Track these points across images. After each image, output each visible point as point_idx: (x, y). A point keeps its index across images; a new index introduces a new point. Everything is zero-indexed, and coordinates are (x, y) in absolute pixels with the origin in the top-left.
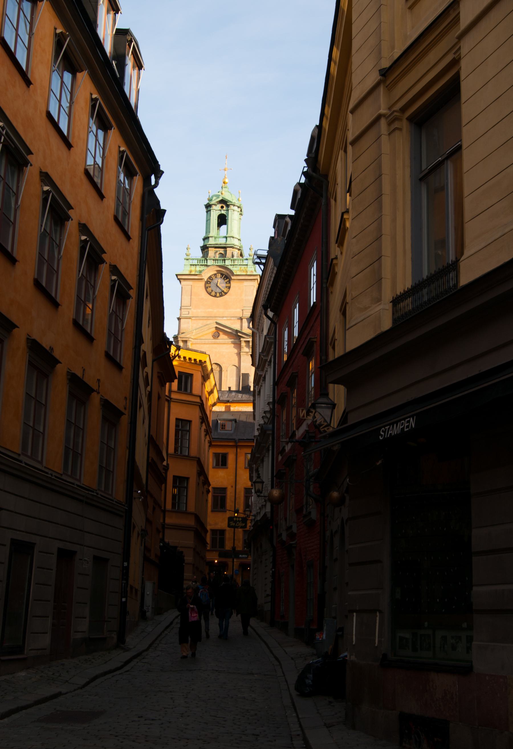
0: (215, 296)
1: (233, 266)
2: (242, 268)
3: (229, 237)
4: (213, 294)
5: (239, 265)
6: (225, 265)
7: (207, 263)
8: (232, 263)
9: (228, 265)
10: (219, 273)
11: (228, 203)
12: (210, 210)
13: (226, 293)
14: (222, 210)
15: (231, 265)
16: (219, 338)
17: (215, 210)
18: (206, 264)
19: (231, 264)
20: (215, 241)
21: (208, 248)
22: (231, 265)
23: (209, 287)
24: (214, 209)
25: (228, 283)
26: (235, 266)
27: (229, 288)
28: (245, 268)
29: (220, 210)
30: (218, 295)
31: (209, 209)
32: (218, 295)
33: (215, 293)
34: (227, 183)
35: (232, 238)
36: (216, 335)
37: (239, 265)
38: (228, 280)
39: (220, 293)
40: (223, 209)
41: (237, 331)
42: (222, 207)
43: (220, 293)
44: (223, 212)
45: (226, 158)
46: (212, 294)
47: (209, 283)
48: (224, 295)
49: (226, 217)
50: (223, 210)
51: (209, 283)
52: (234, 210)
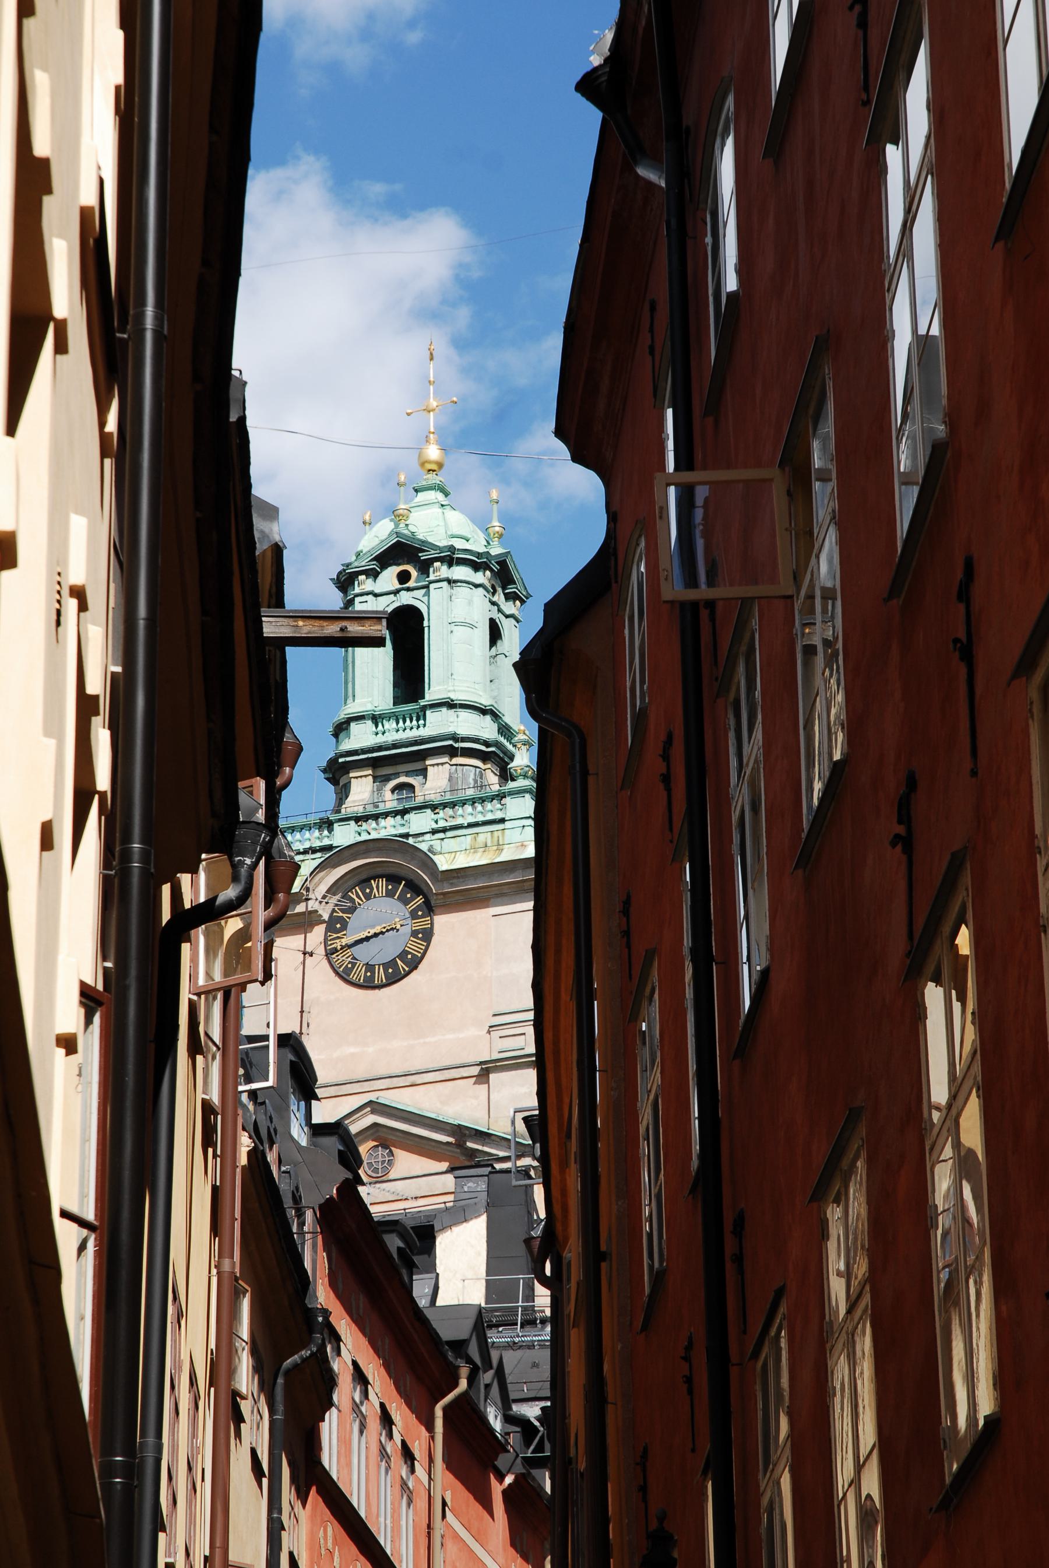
0: (369, 985)
1: (441, 835)
2: (481, 838)
5: (471, 825)
6: (407, 836)
9: (423, 834)
10: (382, 876)
11: (423, 556)
13: (414, 964)
15: (434, 832)
16: (392, 1175)
18: (326, 842)
19: (435, 826)
20: (377, 734)
22: (434, 832)
24: (367, 594)
25: (420, 913)
26: (449, 834)
27: (427, 935)
28: (496, 834)
29: (396, 592)
32: (380, 975)
33: (366, 972)
34: (440, 465)
35: (444, 710)
36: (380, 1159)
37: (471, 825)
38: (419, 900)
40: (407, 585)
41: (461, 1132)
42: (404, 577)
43: (386, 966)
44: (406, 599)
45: (432, 359)
46: (353, 977)
47: (338, 926)
49: (423, 619)
50: (408, 589)
51: (338, 926)
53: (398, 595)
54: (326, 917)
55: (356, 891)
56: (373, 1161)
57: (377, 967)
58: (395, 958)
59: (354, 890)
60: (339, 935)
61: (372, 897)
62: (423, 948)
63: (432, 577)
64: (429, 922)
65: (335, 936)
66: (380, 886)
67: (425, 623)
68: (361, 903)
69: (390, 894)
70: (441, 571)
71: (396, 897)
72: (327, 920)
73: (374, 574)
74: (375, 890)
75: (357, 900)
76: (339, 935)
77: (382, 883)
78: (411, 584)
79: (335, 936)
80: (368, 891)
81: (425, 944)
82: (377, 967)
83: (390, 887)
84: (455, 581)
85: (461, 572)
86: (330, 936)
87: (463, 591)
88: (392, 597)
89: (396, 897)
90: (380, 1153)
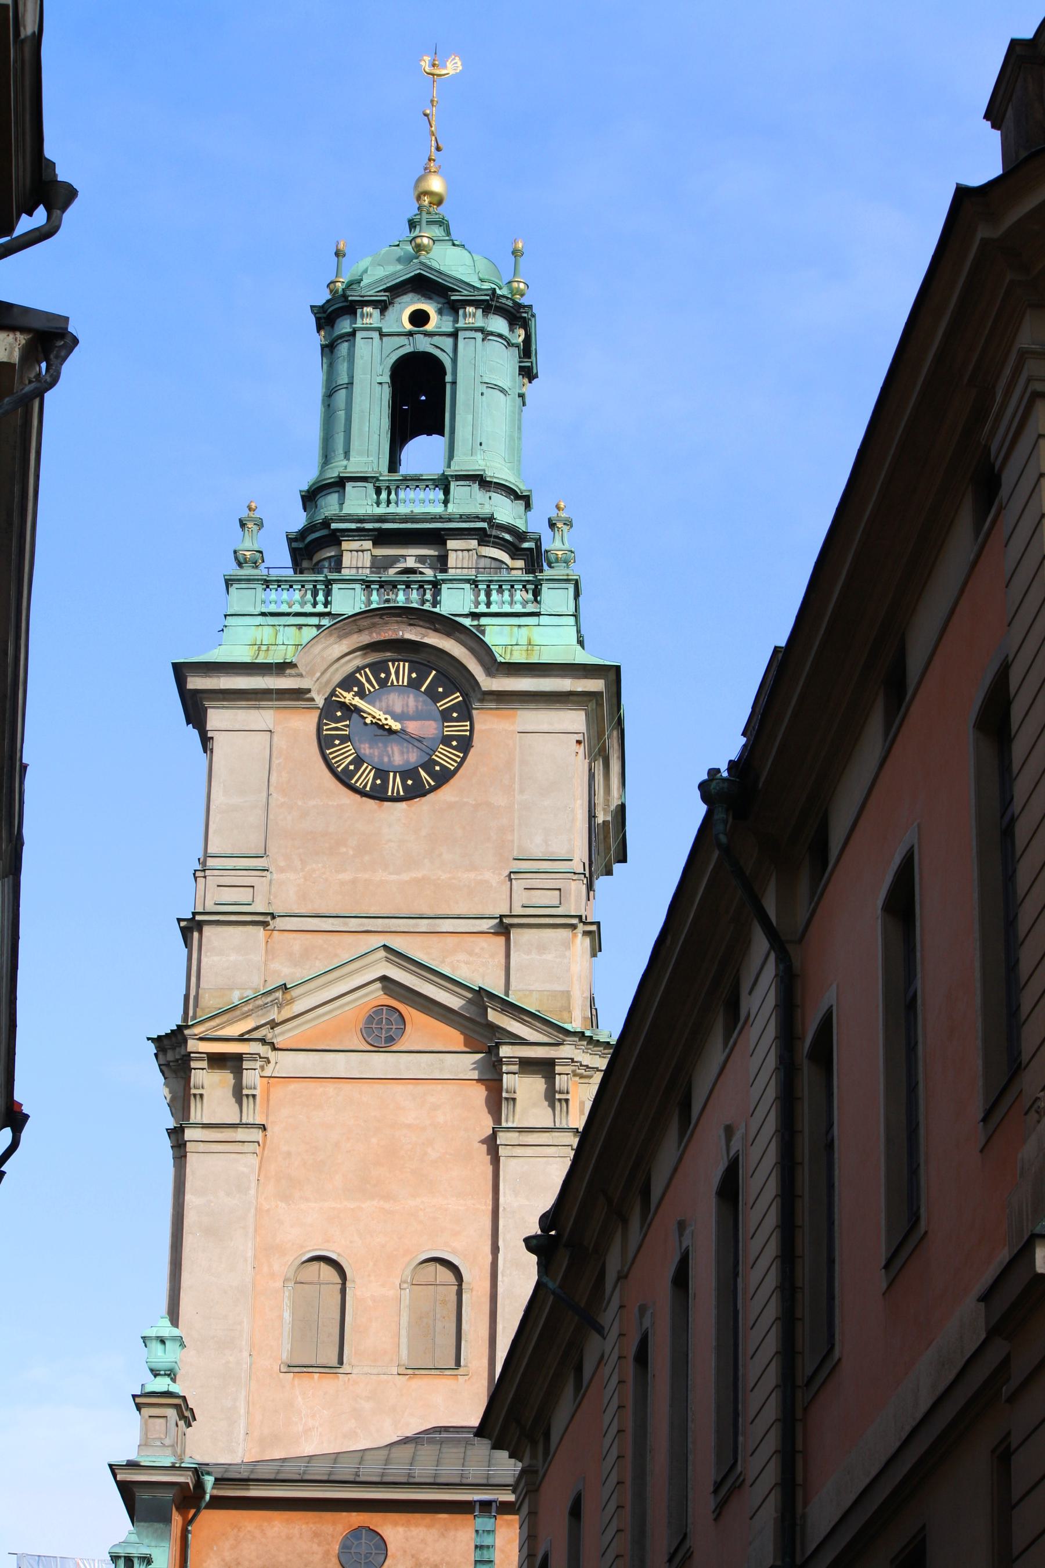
0: (378, 794)
3: (459, 478)
4: (365, 778)
7: (326, 604)
8: (477, 604)
10: (404, 661)
12: (353, 334)
13: (444, 777)
14: (419, 333)
17: (375, 335)
18: (320, 608)
21: (334, 539)
23: (337, 737)
25: (455, 715)
27: (465, 744)
29: (410, 334)
30: (396, 785)
31: (344, 326)
32: (396, 785)
33: (375, 778)
38: (457, 698)
39: (405, 775)
42: (419, 318)
43: (405, 775)
44: (423, 344)
48: (433, 789)
50: (427, 334)
52: (486, 334)
53: (411, 338)
54: (320, 701)
55: (366, 673)
56: (374, 1026)
57: (391, 774)
58: (417, 767)
59: (362, 672)
60: (339, 725)
61: (389, 684)
62: (459, 760)
63: (460, 324)
64: (468, 728)
65: (334, 725)
66: (401, 672)
67: (448, 378)
68: (372, 690)
69: (415, 685)
70: (473, 317)
71: (423, 689)
72: (321, 706)
73: (383, 307)
74: (393, 676)
75: (367, 685)
76: (339, 725)
77: (405, 667)
78: (430, 327)
79: (334, 725)
80: (383, 675)
81: (461, 755)
82: (391, 774)
83: (414, 675)
84: (492, 334)
85: (498, 324)
86: (327, 724)
87: (496, 347)
88: (403, 340)
89: (423, 689)
90: (384, 1016)
